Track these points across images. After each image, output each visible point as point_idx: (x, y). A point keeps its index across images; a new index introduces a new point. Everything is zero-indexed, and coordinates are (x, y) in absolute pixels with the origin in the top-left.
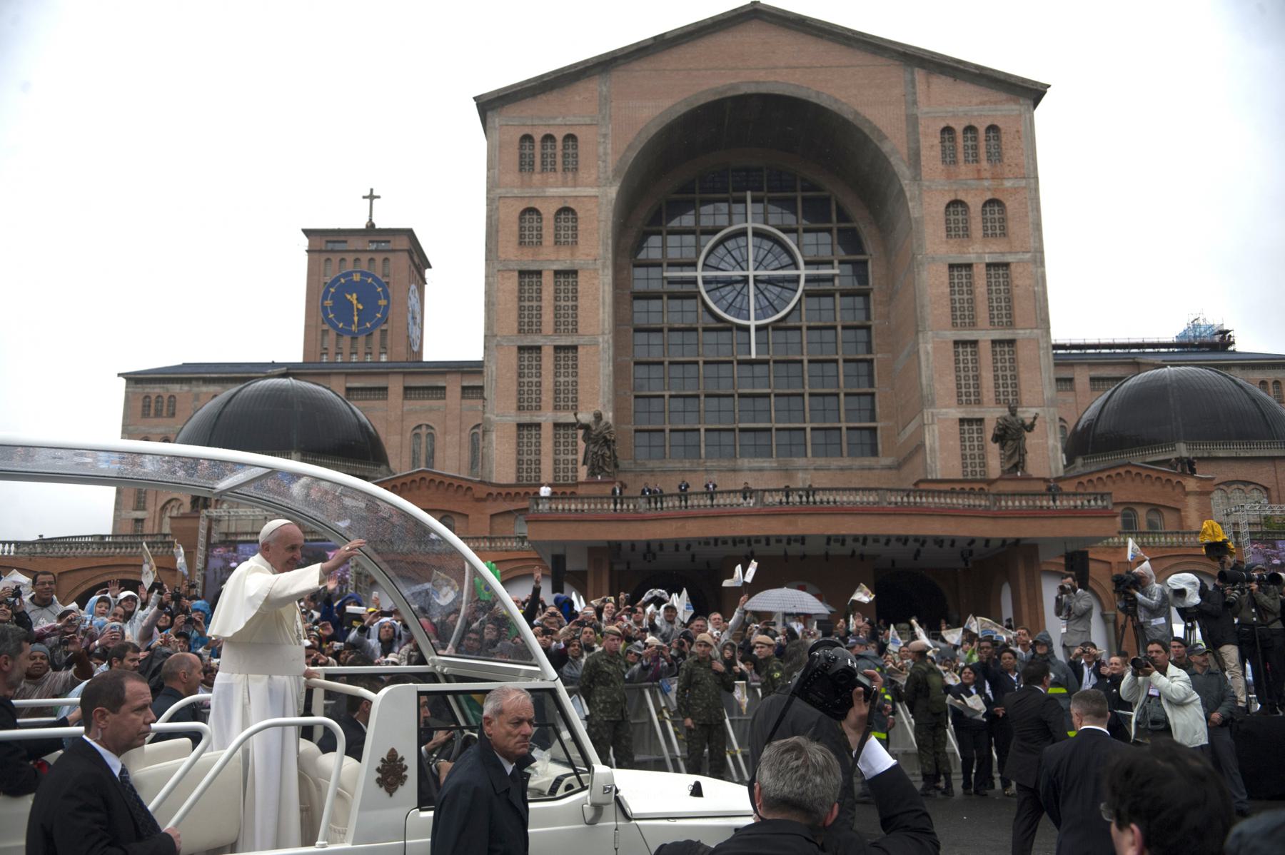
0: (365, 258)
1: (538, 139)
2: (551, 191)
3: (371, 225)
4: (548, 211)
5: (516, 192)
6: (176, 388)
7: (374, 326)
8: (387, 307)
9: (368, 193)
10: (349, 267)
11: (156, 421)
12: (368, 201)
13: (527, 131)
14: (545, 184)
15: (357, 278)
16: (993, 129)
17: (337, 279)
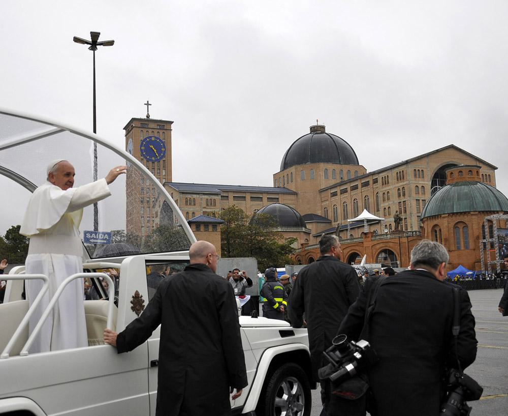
0: (156, 131)
1: (417, 170)
2: (420, 182)
3: (148, 116)
4: (420, 187)
5: (414, 182)
6: (195, 196)
7: (161, 158)
8: (165, 151)
9: (146, 103)
10: (151, 134)
11: (190, 206)
12: (146, 106)
13: (415, 168)
14: (419, 181)
15: (153, 139)
16: (489, 175)
17: (146, 139)
